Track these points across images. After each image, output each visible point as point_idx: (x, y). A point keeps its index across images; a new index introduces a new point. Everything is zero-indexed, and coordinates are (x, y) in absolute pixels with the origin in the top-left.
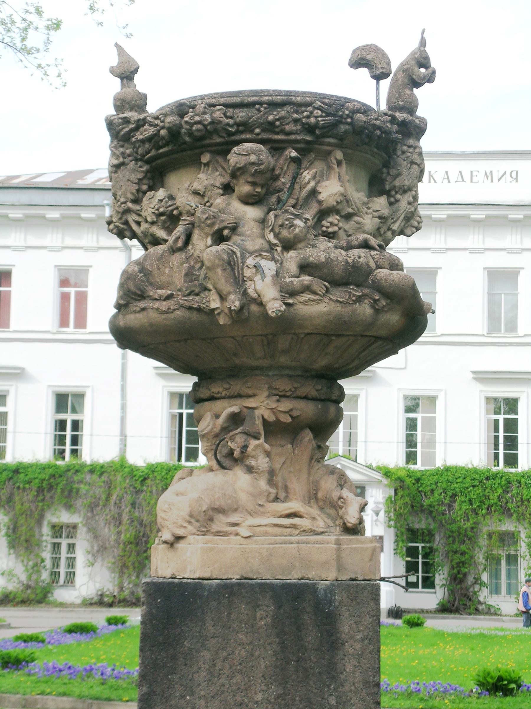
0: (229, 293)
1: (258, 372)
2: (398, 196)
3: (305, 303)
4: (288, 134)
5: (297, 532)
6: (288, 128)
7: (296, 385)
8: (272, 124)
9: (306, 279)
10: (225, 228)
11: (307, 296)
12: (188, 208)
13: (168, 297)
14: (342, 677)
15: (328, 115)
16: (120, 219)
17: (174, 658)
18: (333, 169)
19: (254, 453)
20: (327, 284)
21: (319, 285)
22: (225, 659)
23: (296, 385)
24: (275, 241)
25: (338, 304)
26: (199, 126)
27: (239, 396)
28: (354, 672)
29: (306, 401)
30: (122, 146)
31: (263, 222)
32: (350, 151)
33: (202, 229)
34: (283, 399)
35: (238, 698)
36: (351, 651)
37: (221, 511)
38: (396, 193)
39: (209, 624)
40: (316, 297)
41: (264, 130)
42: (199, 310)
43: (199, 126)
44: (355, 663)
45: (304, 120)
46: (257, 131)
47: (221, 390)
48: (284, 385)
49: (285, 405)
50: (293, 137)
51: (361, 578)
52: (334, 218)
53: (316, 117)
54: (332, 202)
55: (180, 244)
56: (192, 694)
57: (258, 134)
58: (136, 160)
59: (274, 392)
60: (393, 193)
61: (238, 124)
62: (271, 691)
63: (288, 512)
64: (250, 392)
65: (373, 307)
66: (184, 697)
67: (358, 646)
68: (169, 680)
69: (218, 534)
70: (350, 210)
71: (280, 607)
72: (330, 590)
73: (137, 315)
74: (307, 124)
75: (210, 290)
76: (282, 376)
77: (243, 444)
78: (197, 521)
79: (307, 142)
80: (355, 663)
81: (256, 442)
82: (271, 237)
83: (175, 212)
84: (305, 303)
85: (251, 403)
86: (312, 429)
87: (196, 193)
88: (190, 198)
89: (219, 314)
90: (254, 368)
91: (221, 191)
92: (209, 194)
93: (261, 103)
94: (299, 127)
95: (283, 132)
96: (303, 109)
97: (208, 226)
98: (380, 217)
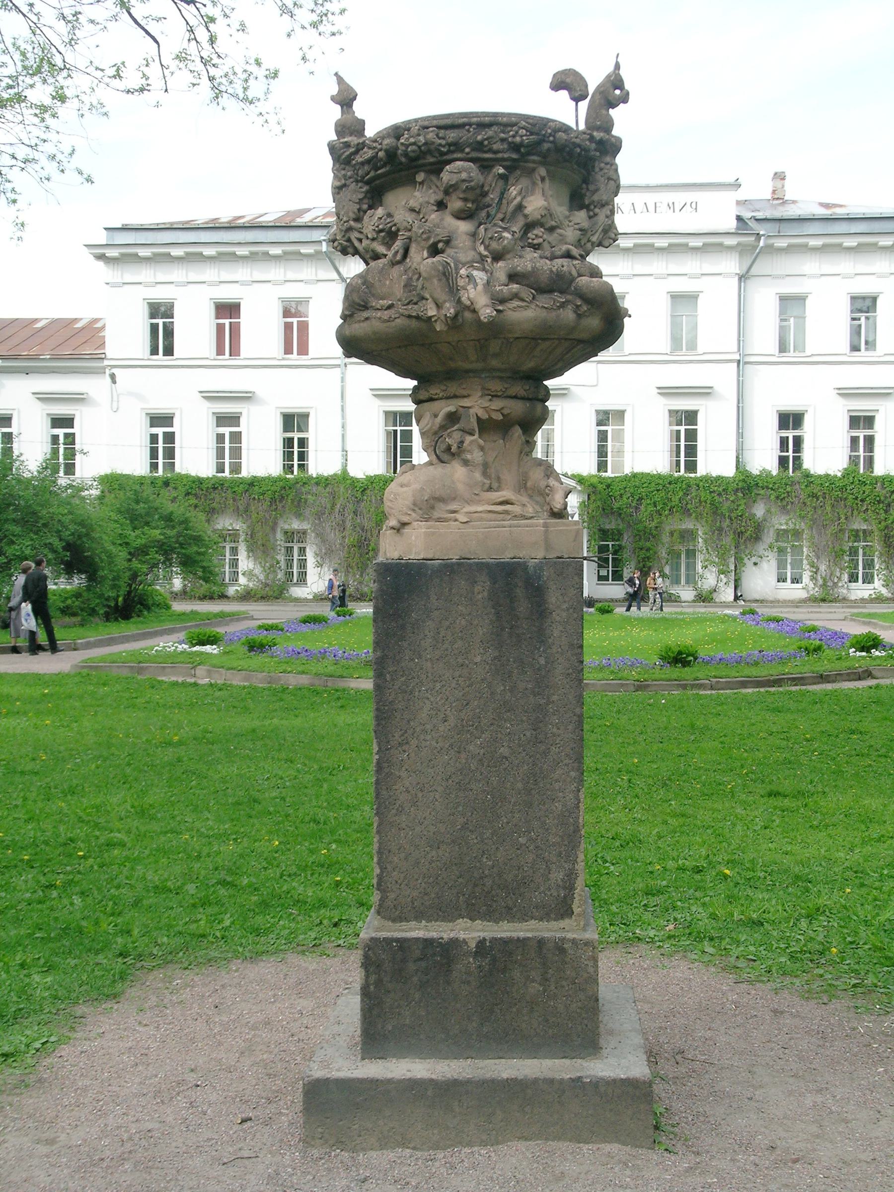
0: (445, 301)
1: (471, 375)
2: (597, 210)
3: (514, 309)
4: (496, 152)
5: (510, 517)
6: (495, 147)
7: (506, 386)
8: (481, 143)
9: (515, 287)
10: (440, 241)
11: (516, 303)
12: (405, 224)
13: (390, 307)
14: (550, 641)
15: (532, 134)
16: (344, 236)
17: (403, 627)
18: (537, 184)
21: (526, 293)
22: (449, 627)
23: (506, 386)
24: (486, 253)
25: (544, 310)
26: (414, 147)
27: (455, 397)
28: (560, 637)
30: (344, 169)
31: (474, 235)
32: (552, 168)
33: (419, 243)
34: (494, 399)
35: (460, 660)
36: (558, 618)
38: (595, 207)
39: (433, 598)
40: (524, 304)
41: (473, 150)
42: (417, 318)
43: (414, 147)
44: (561, 628)
45: (510, 139)
46: (467, 150)
47: (438, 391)
48: (496, 386)
49: (497, 404)
50: (500, 155)
51: (566, 556)
52: (538, 231)
53: (522, 136)
54: (537, 216)
55: (399, 257)
56: (420, 657)
57: (468, 154)
58: (357, 181)
59: (486, 392)
60: (592, 207)
61: (450, 145)
62: (488, 654)
63: (501, 499)
64: (465, 393)
65: (575, 312)
66: (413, 660)
67: (564, 614)
68: (399, 646)
69: (439, 520)
70: (553, 223)
71: (494, 583)
72: (540, 567)
73: (362, 324)
74: (513, 143)
75: (427, 299)
76: (494, 377)
77: (459, 440)
78: (420, 509)
79: (514, 160)
80: (561, 628)
81: (472, 438)
82: (482, 249)
83: (393, 229)
84: (514, 309)
85: (466, 402)
87: (412, 210)
88: (407, 215)
89: (436, 321)
90: (467, 371)
91: (435, 208)
92: (423, 210)
93: (470, 125)
94: (506, 146)
95: (490, 151)
96: (509, 128)
97: (424, 240)
98: (580, 230)
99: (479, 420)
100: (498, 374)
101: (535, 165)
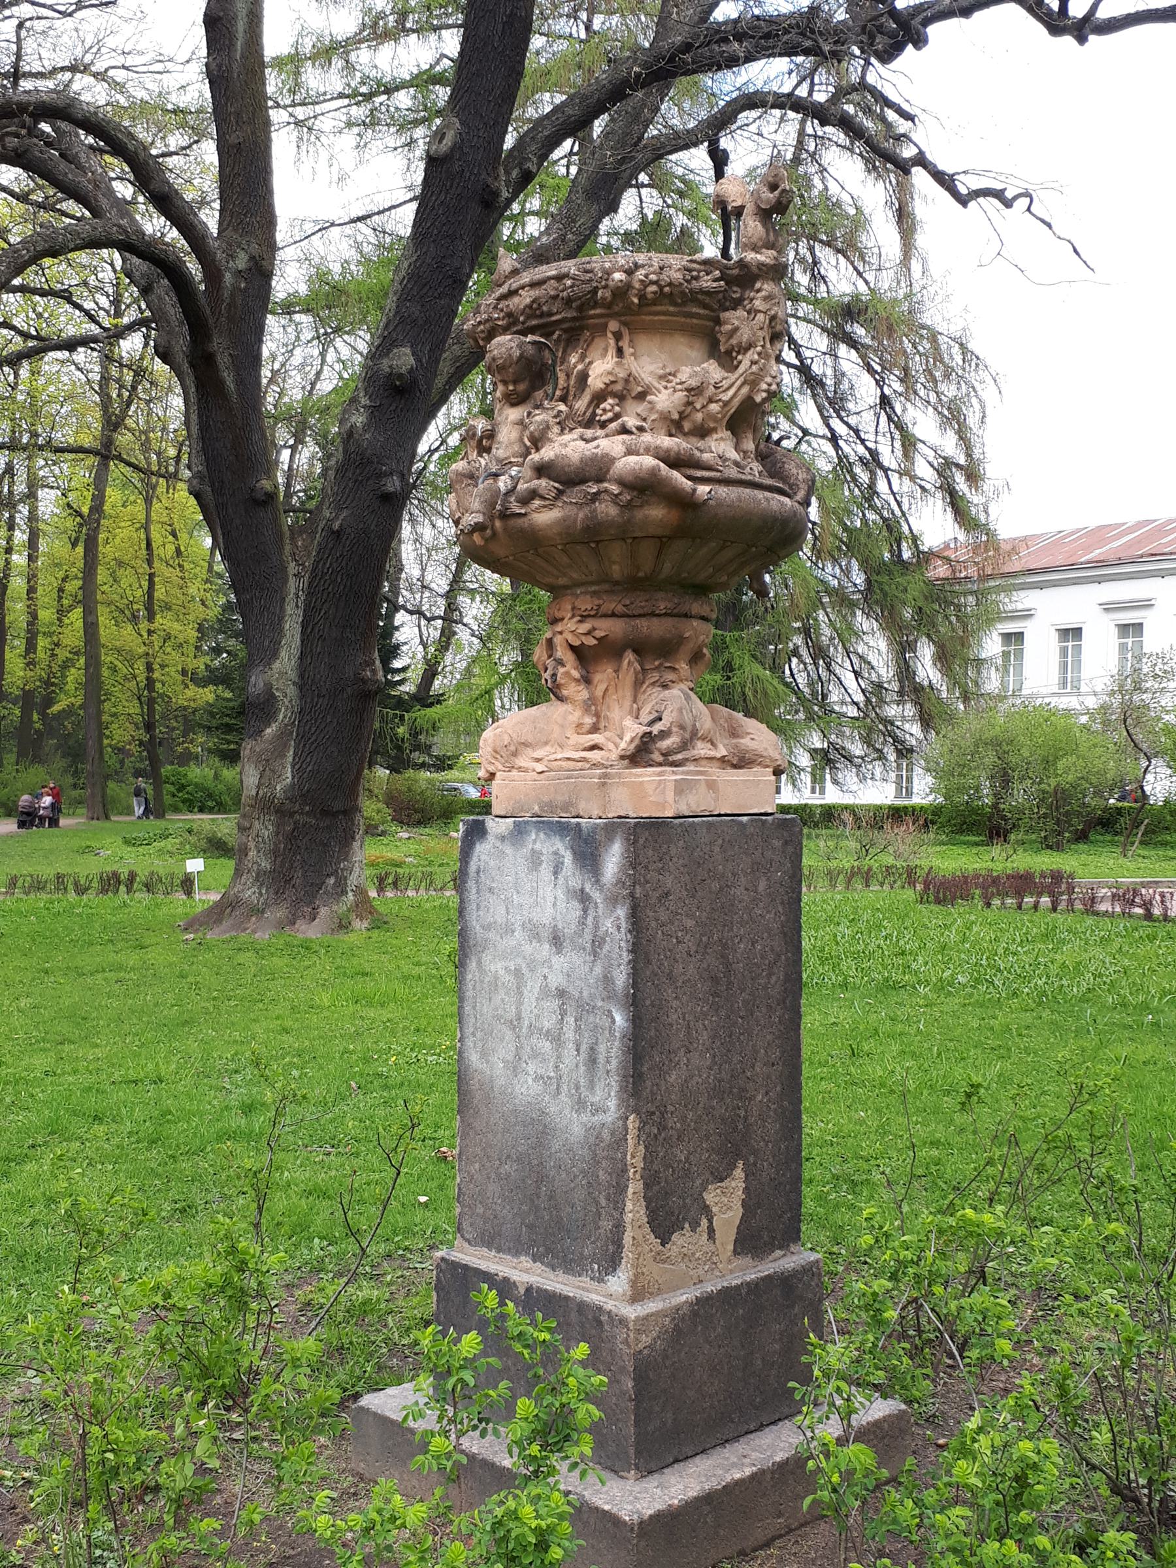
1: (569, 591)
2: (740, 357)
4: (551, 314)
5: (588, 766)
7: (597, 602)
19: (563, 681)
20: (556, 485)
29: (616, 619)
32: (628, 318)
37: (526, 745)
40: (548, 502)
48: (586, 604)
50: (554, 318)
57: (523, 323)
60: (734, 354)
69: (520, 769)
70: (640, 389)
76: (586, 593)
79: (573, 319)
84: (537, 511)
86: (635, 651)
95: (542, 315)
98: (688, 390)
99: (573, 648)
100: (593, 588)
101: (602, 320)
